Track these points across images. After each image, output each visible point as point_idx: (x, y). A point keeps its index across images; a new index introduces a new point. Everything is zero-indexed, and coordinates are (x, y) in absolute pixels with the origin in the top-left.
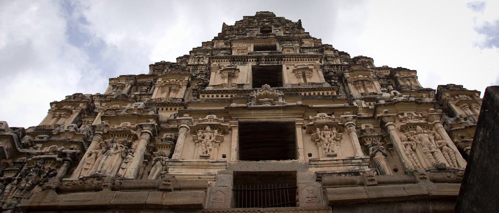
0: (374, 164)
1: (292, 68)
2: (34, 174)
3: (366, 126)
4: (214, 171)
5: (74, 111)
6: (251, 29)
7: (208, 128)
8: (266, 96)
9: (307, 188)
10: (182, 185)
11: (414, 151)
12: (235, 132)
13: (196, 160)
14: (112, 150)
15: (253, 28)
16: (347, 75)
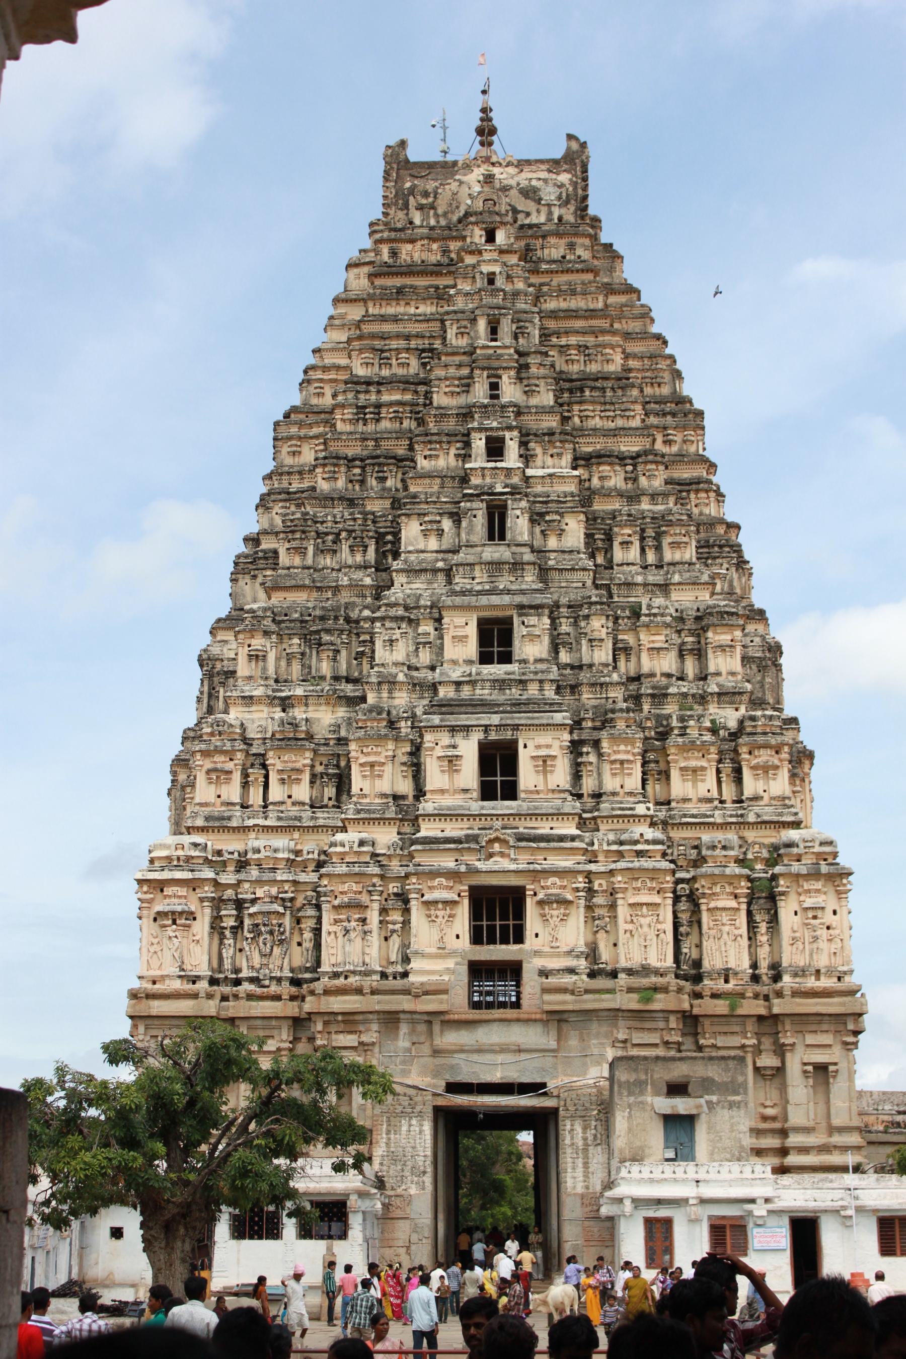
0: (592, 954)
1: (531, 751)
2: (268, 936)
3: (600, 885)
4: (450, 963)
5: (230, 766)
6: (468, 504)
7: (440, 906)
8: (497, 839)
9: (530, 983)
10: (428, 988)
11: (632, 936)
12: (466, 902)
13: (434, 950)
14: (353, 935)
15: (469, 497)
16: (605, 744)
